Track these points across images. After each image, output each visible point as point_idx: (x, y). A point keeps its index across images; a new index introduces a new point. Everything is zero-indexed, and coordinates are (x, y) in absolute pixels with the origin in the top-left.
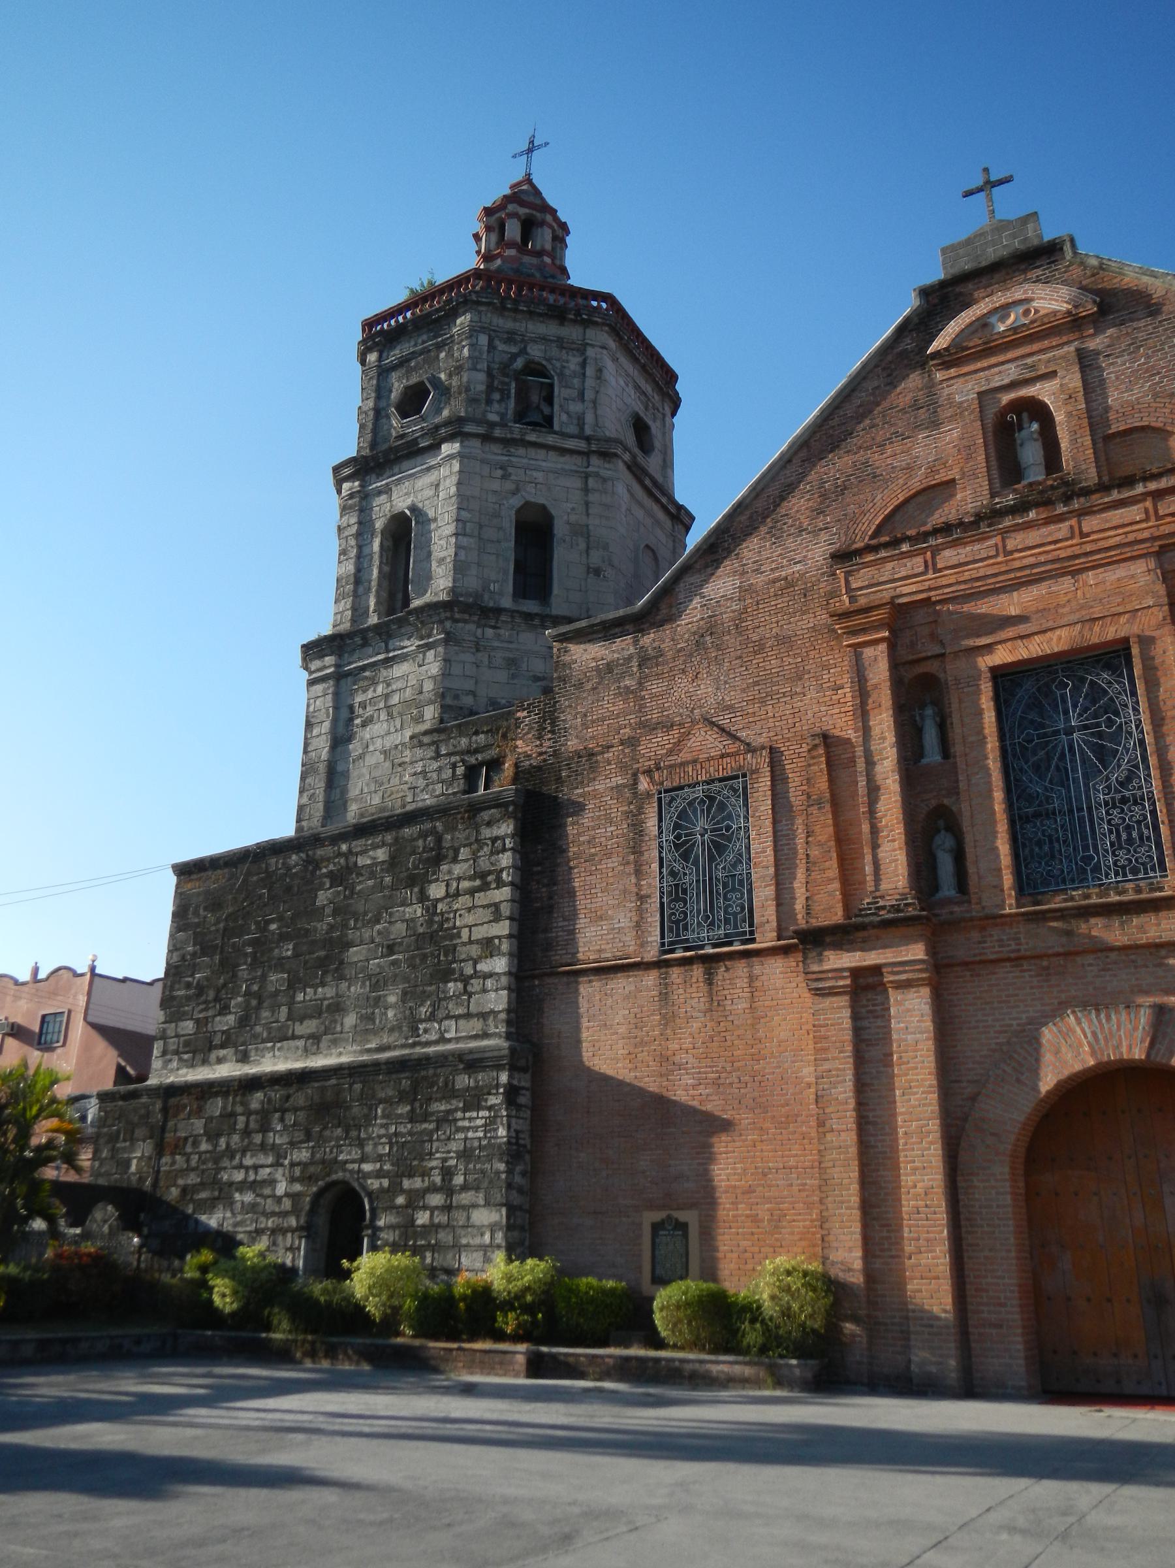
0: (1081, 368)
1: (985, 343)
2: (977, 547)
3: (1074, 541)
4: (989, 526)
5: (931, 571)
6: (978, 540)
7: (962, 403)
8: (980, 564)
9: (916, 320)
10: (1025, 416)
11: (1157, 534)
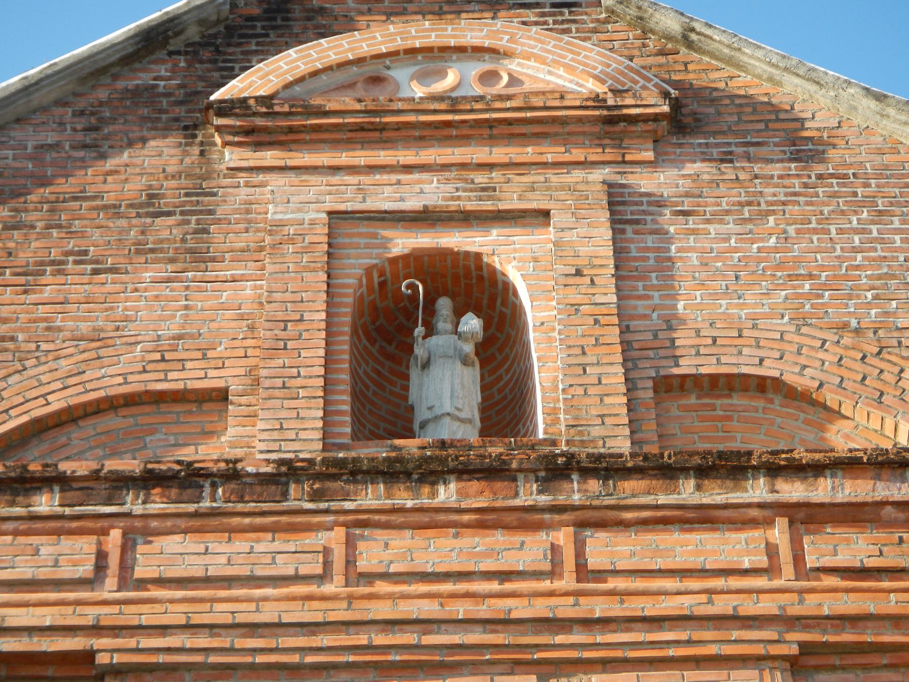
0: (613, 222)
1: (367, 112)
2: (265, 544)
3: (559, 585)
4: (315, 496)
5: (111, 582)
6: (273, 529)
7: (281, 224)
8: (268, 591)
9: (193, 33)
10: (444, 305)
11: (795, 610)
